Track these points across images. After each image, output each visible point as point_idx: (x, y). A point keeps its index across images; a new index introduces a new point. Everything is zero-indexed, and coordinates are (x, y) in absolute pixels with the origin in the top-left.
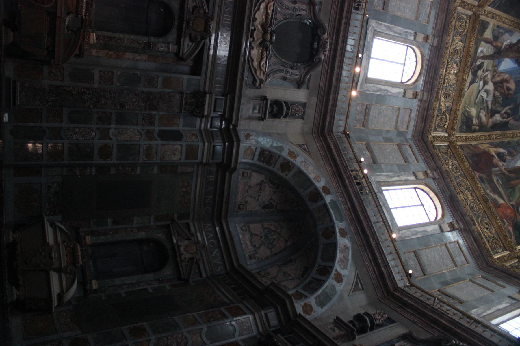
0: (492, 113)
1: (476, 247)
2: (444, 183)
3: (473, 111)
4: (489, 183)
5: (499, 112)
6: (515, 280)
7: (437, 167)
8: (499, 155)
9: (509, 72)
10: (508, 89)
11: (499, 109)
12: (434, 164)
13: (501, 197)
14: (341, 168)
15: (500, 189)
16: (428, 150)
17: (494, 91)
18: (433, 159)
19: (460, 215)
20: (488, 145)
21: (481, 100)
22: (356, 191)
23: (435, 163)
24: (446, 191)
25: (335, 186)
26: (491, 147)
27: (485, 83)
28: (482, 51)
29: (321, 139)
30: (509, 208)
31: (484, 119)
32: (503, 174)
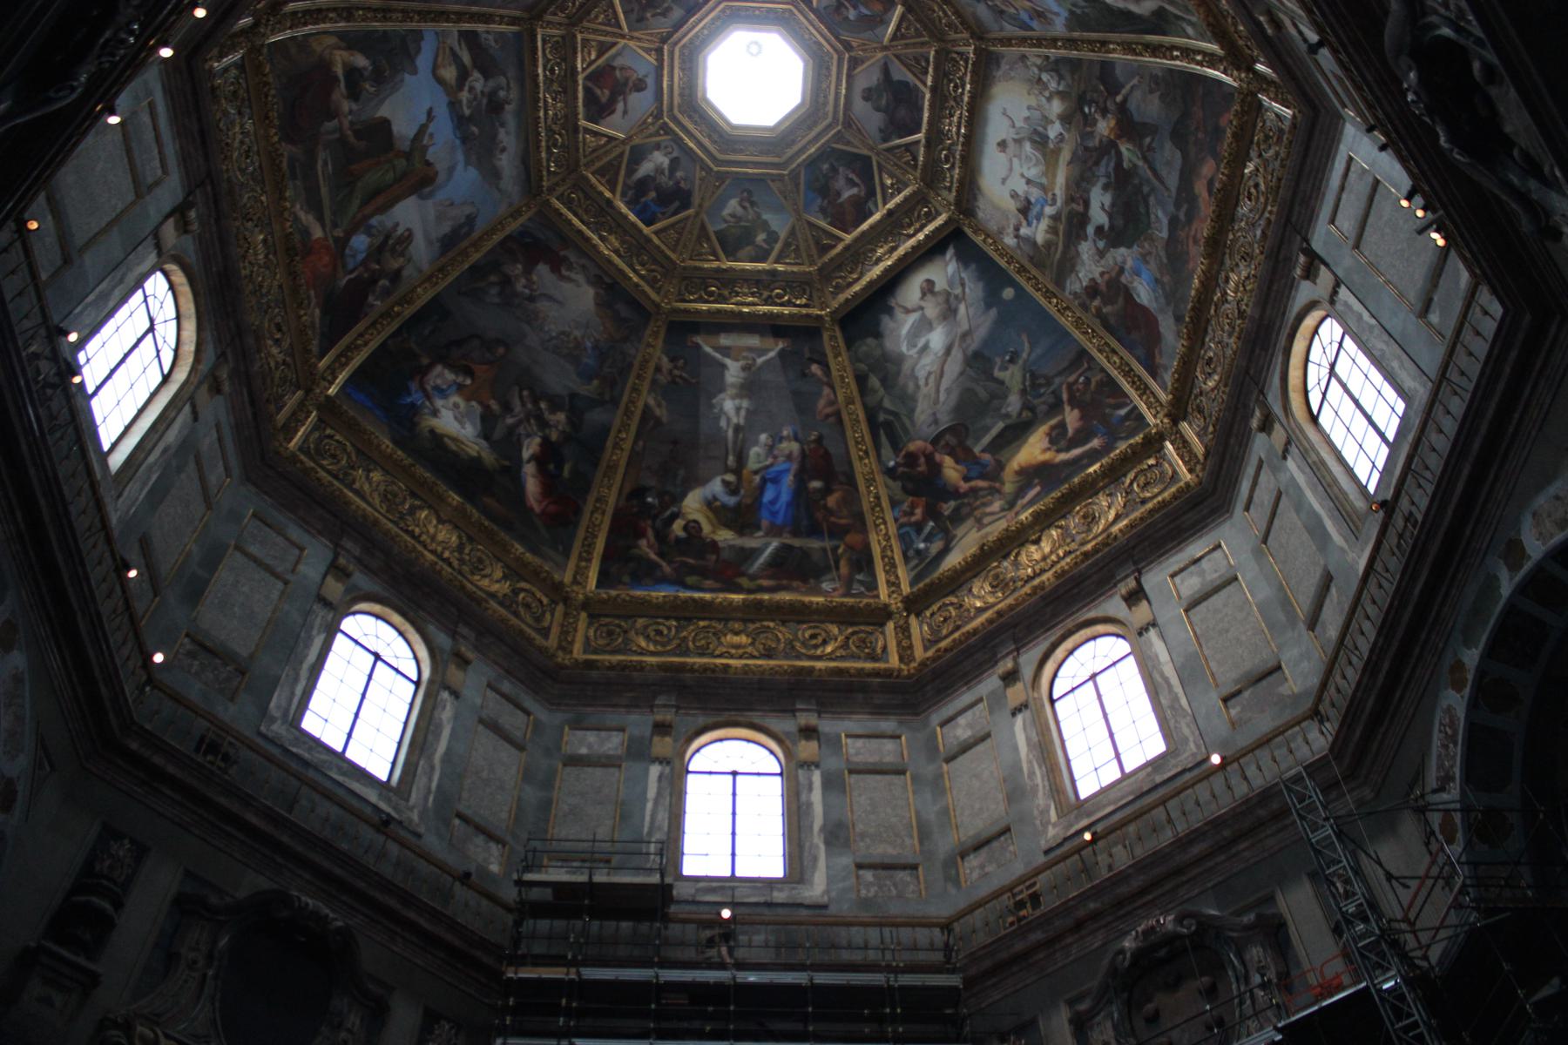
8: (352, 73)
15: (324, 191)
26: (339, 48)
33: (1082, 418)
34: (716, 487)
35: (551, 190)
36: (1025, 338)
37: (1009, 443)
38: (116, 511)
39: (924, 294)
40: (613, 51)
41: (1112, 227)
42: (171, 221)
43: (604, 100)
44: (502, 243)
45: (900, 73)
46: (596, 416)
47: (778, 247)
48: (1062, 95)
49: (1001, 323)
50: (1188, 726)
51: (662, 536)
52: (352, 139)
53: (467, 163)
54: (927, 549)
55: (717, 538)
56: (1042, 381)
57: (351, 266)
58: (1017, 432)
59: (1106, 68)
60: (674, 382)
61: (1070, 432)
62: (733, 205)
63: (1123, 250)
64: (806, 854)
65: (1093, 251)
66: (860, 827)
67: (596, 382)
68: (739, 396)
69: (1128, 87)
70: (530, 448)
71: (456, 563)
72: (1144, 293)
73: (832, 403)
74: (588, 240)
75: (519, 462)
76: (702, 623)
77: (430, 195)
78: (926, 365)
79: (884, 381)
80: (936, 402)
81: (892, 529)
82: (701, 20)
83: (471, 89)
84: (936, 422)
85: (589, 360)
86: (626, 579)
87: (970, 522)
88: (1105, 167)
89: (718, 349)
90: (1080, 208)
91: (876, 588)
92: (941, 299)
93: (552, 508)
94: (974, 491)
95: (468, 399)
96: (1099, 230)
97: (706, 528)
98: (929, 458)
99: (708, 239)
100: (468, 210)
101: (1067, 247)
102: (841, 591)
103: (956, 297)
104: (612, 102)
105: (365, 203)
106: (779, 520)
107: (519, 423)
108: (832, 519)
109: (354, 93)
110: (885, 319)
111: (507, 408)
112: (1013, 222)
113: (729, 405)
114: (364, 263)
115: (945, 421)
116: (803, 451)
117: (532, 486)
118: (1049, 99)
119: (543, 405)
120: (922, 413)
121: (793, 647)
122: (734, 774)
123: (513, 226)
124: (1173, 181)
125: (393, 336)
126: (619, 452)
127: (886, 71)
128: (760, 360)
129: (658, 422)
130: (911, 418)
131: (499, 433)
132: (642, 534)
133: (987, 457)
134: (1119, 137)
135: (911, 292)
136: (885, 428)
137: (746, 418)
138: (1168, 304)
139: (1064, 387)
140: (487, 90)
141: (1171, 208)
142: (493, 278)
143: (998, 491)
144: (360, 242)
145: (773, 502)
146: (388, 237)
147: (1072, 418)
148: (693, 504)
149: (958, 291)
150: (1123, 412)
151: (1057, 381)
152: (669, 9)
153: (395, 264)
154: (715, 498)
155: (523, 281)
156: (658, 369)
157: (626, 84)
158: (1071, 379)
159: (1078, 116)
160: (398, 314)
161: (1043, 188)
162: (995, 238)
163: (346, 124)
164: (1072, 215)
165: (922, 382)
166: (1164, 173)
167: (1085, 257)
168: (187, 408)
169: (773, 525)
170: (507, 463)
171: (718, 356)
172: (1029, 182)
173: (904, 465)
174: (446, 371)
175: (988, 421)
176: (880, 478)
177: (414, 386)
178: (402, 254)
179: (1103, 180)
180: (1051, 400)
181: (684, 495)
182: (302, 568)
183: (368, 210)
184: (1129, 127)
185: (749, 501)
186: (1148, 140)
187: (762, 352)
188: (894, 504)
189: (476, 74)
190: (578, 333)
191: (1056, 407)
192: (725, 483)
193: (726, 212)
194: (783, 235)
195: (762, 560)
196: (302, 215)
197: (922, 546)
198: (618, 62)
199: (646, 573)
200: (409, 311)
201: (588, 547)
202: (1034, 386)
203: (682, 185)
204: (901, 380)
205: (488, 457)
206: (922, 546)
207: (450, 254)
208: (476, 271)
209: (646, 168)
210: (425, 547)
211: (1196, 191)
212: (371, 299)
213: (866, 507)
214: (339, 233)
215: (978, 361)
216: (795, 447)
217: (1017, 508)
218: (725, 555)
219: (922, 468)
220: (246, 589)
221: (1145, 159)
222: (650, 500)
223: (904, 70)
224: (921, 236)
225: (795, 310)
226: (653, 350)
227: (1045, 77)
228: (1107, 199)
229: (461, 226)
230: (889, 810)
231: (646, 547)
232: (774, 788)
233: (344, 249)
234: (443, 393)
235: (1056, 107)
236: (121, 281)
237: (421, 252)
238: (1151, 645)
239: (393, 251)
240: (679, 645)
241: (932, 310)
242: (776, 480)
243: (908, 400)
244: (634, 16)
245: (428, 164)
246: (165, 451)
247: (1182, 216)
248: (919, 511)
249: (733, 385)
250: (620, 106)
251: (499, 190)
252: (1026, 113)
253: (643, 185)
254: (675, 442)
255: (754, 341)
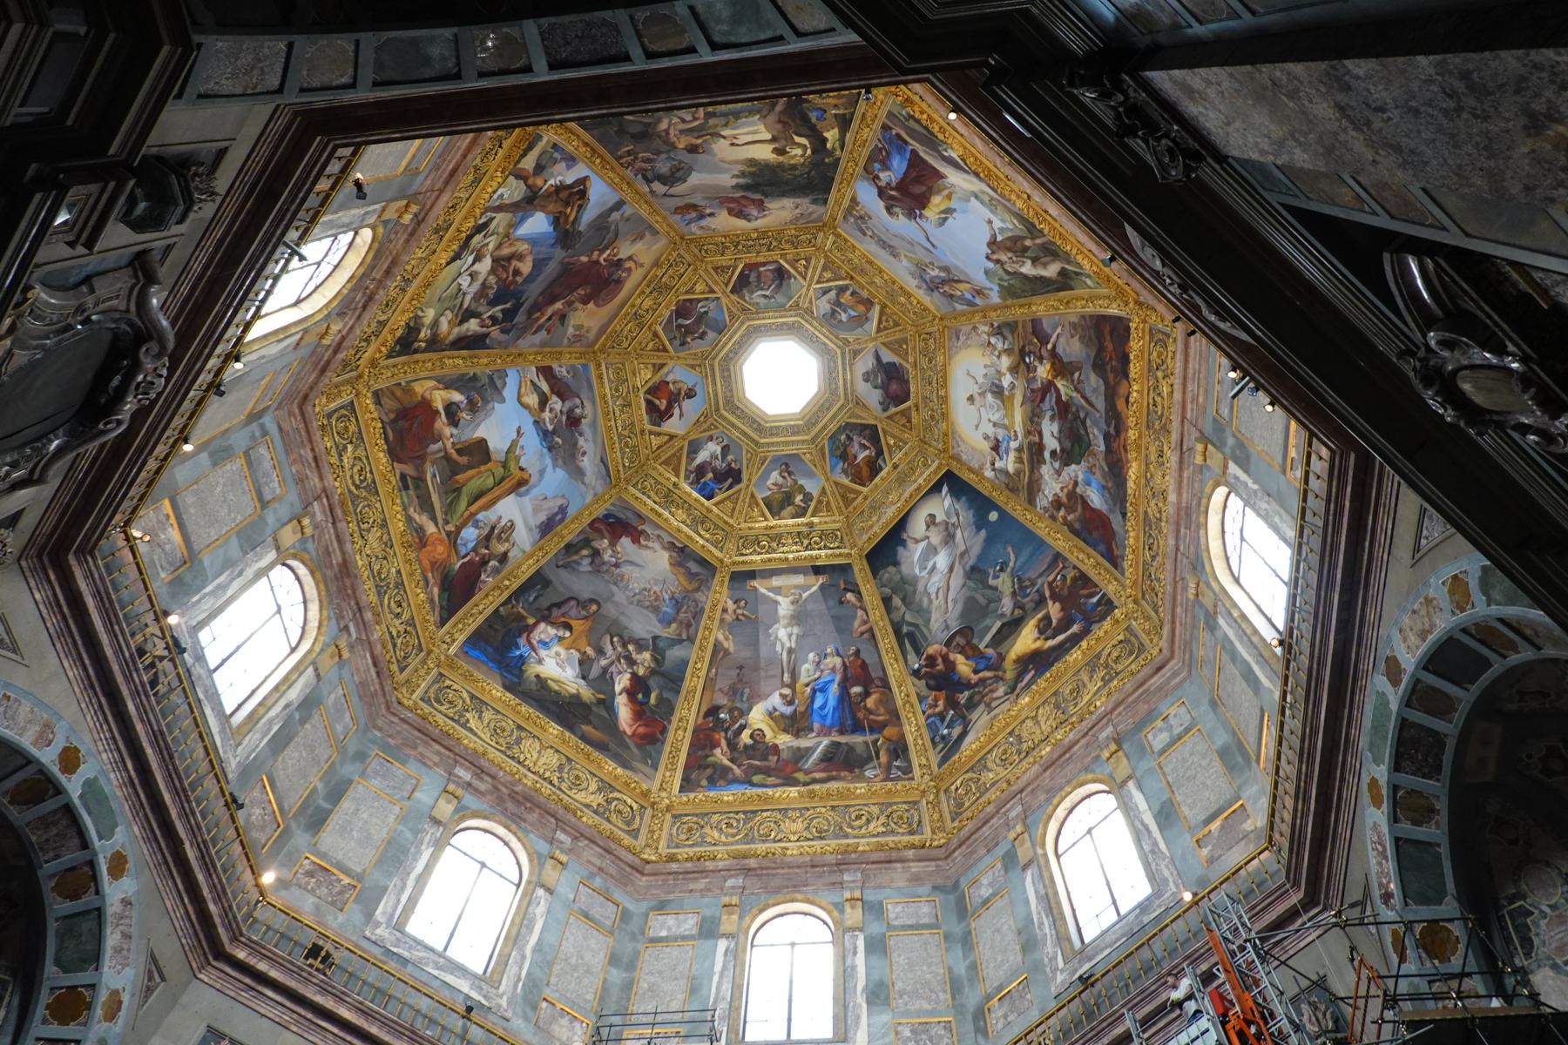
0: (468, 314)
1: (374, 675)
2: (332, 531)
3: (430, 314)
4: (417, 487)
5: (477, 315)
6: (437, 747)
7: (324, 490)
9: (533, 241)
10: (517, 272)
11: (481, 309)
12: (317, 480)
13: (434, 519)
14: (115, 668)
15: (435, 498)
16: (311, 441)
17: (489, 274)
18: (318, 467)
19: (355, 607)
20: (432, 383)
21: (455, 292)
22: (156, 728)
23: (321, 478)
24: (334, 551)
25: (91, 724)
27: (477, 259)
28: (502, 195)
29: (52, 577)
30: (441, 541)
31: (444, 326)
32: (447, 457)
33: (1062, 610)
34: (775, 700)
35: (628, 481)
36: (1010, 550)
37: (1007, 638)
38: (235, 757)
39: (928, 527)
40: (665, 370)
41: (1062, 450)
42: (289, 528)
43: (663, 408)
44: (591, 525)
45: (888, 357)
46: (675, 654)
47: (813, 505)
48: (1008, 352)
49: (989, 542)
50: (1167, 867)
51: (732, 745)
52: (455, 455)
53: (555, 466)
54: (950, 734)
55: (777, 742)
56: (1028, 583)
57: (463, 551)
58: (1012, 627)
59: (1036, 323)
60: (737, 619)
61: (1054, 622)
62: (775, 476)
63: (1073, 466)
64: (850, 1014)
65: (1052, 471)
66: (899, 985)
67: (674, 626)
68: (790, 625)
69: (1055, 335)
70: (622, 682)
71: (556, 781)
72: (1096, 499)
73: (865, 622)
74: (660, 515)
75: (613, 695)
76: (765, 814)
77: (527, 492)
78: (936, 582)
79: (903, 600)
80: (946, 611)
81: (922, 719)
82: (730, 339)
83: (551, 410)
84: (947, 627)
85: (667, 609)
86: (704, 783)
87: (982, 707)
88: (1050, 400)
89: (771, 589)
90: (1037, 439)
91: (911, 771)
92: (942, 528)
93: (641, 730)
94: (983, 681)
95: (568, 649)
96: (1053, 453)
97: (769, 734)
98: (945, 658)
99: (758, 505)
100: (559, 502)
101: (1032, 472)
102: (881, 777)
103: (953, 525)
104: (670, 407)
105: (470, 504)
106: (828, 722)
107: (613, 663)
108: (872, 717)
109: (453, 420)
110: (900, 549)
111: (600, 652)
112: (989, 459)
113: (782, 633)
114: (474, 550)
115: (955, 626)
116: (844, 663)
117: (624, 712)
118: (999, 357)
119: (631, 648)
120: (936, 623)
121: (841, 828)
122: (793, 944)
123: (599, 511)
124: (1100, 403)
125: (504, 604)
126: (694, 681)
127: (878, 357)
128: (805, 595)
129: (727, 652)
130: (929, 629)
131: (595, 672)
132: (715, 745)
133: (990, 651)
134: (1055, 377)
135: (918, 526)
136: (908, 638)
137: (797, 641)
138: (1115, 504)
139: (1046, 586)
140: (565, 410)
141: (1104, 426)
142: (585, 552)
143: (1002, 679)
144: (470, 534)
145: (822, 707)
146: (493, 528)
147: (1054, 610)
148: (757, 717)
149: (954, 520)
150: (1095, 600)
151: (1040, 581)
152: (704, 333)
153: (501, 548)
154: (775, 709)
155: (610, 552)
156: (725, 610)
157: (679, 393)
158: (1051, 578)
159: (1022, 366)
160: (507, 587)
161: (1005, 427)
162: (978, 473)
163: (449, 445)
164: (1031, 445)
165: (933, 596)
166: (1093, 399)
167: (1046, 477)
168: (311, 669)
169: (823, 726)
170: (602, 696)
171: (771, 595)
172: (995, 425)
173: (926, 666)
174: (549, 628)
175: (988, 621)
176: (910, 680)
177: (522, 641)
178: (507, 540)
179: (1049, 414)
180: (1036, 597)
181: (750, 709)
182: (417, 795)
183: (473, 508)
184: (1062, 368)
185: (802, 709)
186: (1077, 375)
187: (808, 588)
188: (921, 699)
189: (555, 398)
190: (656, 588)
191: (1040, 602)
192: (783, 696)
193: (769, 482)
194: (815, 494)
195: (815, 756)
196: (416, 517)
197: (946, 732)
198: (670, 378)
199: (719, 776)
200: (516, 584)
201: (673, 757)
202: (1022, 588)
203: (733, 465)
204: (917, 597)
205: (587, 694)
206: (946, 732)
207: (548, 537)
208: (570, 548)
209: (702, 456)
210: (529, 770)
211: (1119, 408)
212: (483, 577)
213: (899, 703)
214: (450, 528)
215: (976, 573)
216: (838, 661)
217: (1017, 691)
218: (784, 755)
219: (940, 667)
220: (365, 816)
221: (1077, 390)
222: (722, 716)
223: (890, 353)
224: (921, 481)
225: (830, 552)
226: (719, 595)
227: (993, 340)
228: (1055, 428)
229: (556, 514)
230: (925, 968)
231: (720, 755)
232: (828, 954)
233: (455, 542)
234: (545, 644)
235: (1006, 362)
236: (240, 574)
237: (523, 537)
238: (1131, 797)
239: (499, 538)
240: (746, 835)
241: (936, 537)
242: (823, 690)
243: (924, 613)
244: (677, 342)
245: (522, 469)
246: (287, 706)
247: (1112, 431)
248: (941, 703)
249: (784, 617)
250: (676, 411)
251: (583, 483)
252: (985, 371)
253: (701, 470)
254: (741, 668)
255: (799, 580)
